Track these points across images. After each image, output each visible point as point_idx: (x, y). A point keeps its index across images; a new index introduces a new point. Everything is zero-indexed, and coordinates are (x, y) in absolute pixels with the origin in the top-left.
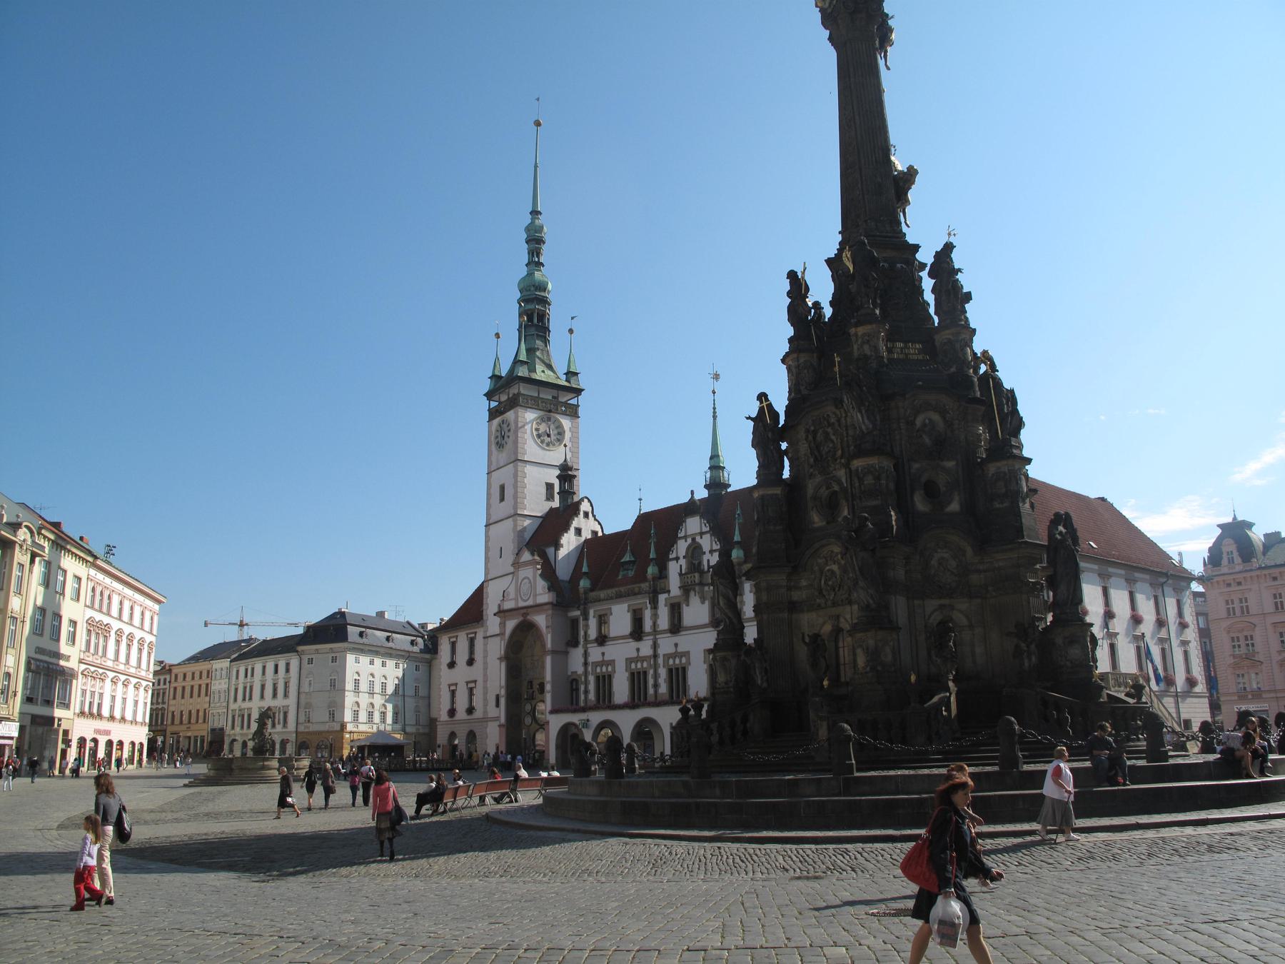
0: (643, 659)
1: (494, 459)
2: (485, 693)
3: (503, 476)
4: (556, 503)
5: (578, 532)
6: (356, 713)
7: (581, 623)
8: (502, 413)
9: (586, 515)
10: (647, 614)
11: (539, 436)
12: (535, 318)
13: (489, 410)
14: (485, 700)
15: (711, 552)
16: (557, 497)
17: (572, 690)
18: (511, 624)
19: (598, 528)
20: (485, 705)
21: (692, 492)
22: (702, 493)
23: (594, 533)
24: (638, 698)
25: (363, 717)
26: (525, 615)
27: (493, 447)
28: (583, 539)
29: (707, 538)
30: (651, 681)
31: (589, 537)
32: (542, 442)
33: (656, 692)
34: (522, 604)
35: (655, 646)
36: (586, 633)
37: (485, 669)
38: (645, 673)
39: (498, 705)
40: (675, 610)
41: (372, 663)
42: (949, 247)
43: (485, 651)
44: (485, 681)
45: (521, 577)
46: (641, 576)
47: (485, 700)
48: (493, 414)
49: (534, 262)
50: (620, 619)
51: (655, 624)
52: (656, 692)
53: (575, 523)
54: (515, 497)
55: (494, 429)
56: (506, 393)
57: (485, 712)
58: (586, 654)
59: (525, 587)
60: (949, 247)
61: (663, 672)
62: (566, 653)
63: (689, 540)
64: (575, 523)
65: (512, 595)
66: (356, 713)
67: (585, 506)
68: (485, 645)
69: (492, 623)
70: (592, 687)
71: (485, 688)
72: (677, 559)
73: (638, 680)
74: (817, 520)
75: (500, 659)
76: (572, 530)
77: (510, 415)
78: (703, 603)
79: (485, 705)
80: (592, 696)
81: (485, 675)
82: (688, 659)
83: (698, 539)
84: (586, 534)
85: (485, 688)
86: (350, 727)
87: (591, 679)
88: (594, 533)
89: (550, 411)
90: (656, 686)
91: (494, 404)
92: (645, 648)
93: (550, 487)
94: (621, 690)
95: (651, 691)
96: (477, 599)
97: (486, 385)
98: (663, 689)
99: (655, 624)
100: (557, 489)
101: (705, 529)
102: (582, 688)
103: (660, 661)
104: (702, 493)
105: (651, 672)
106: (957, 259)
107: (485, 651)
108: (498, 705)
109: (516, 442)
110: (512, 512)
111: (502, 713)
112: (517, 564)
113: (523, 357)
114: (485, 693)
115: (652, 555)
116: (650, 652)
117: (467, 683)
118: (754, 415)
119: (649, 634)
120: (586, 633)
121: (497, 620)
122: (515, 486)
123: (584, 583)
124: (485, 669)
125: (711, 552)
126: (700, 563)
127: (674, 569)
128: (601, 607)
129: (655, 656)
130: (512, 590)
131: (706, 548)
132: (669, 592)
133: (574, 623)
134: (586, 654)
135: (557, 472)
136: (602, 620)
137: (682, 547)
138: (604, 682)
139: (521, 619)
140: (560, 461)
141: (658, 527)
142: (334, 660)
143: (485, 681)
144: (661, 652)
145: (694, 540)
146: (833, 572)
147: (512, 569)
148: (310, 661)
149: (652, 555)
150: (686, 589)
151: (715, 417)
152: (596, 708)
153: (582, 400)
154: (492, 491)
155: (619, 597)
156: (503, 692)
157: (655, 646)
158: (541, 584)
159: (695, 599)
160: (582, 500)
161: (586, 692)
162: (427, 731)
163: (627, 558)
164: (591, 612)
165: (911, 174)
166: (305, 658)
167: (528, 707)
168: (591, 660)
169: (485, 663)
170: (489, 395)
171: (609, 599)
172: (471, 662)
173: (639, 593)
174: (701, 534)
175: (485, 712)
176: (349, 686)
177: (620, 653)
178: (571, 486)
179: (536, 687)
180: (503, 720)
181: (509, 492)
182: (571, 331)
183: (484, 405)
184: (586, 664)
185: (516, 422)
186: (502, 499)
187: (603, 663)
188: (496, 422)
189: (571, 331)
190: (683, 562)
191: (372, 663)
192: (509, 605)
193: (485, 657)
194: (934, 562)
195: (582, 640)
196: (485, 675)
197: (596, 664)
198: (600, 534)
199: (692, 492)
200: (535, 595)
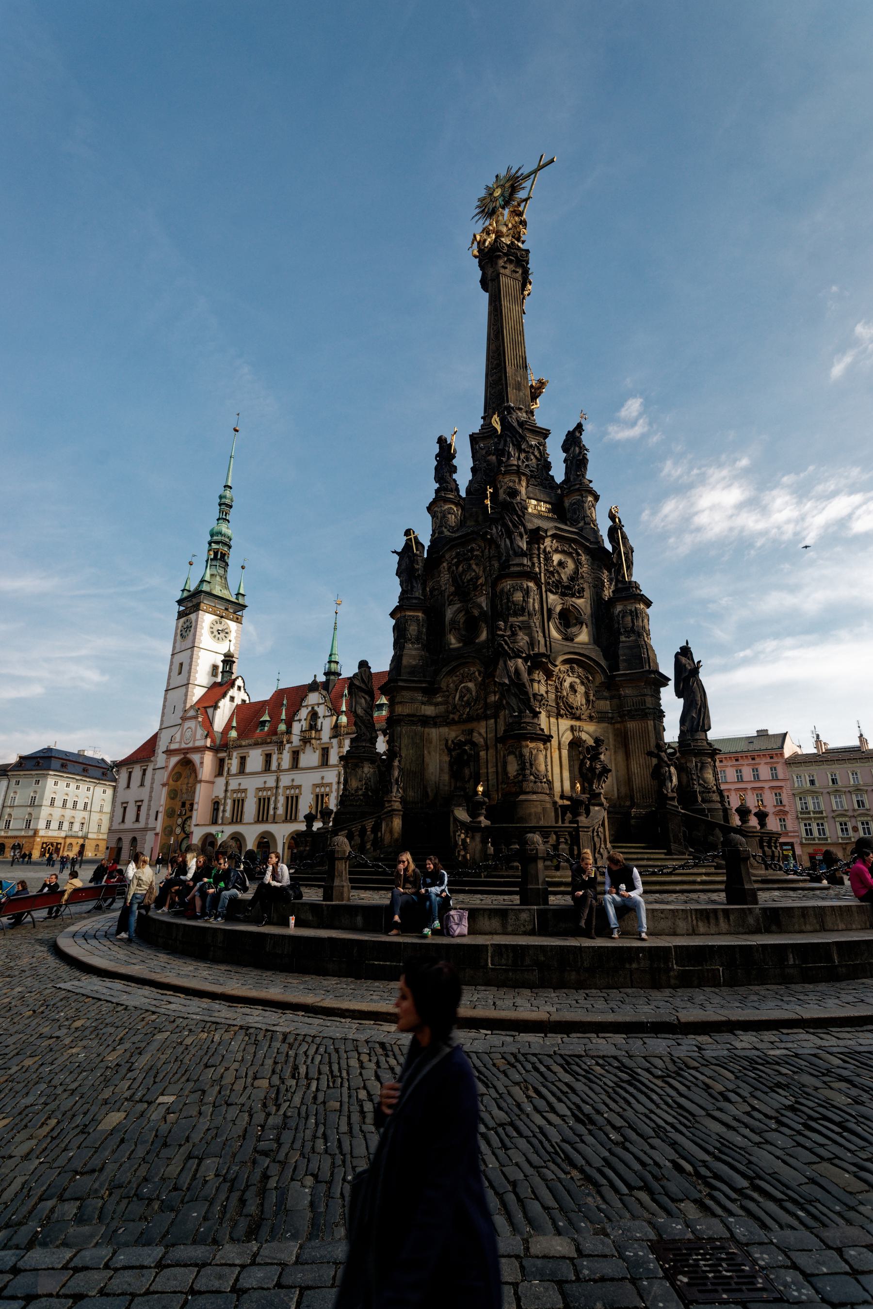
0: (270, 789)
1: (178, 645)
2: (149, 810)
3: (182, 657)
4: (219, 679)
5: (232, 699)
6: (49, 823)
7: (226, 761)
8: (187, 615)
9: (239, 688)
10: (274, 758)
11: (212, 633)
12: (219, 555)
13: (179, 612)
14: (148, 815)
15: (324, 717)
16: (220, 675)
17: (214, 809)
18: (174, 760)
19: (246, 698)
20: (147, 819)
21: (315, 676)
22: (322, 678)
23: (244, 701)
24: (262, 816)
25: (54, 825)
26: (187, 753)
27: (179, 637)
28: (235, 704)
29: (322, 707)
30: (272, 806)
31: (240, 703)
32: (215, 637)
33: (275, 813)
34: (184, 746)
35: (278, 780)
36: (229, 769)
37: (151, 792)
38: (269, 799)
41: (68, 786)
42: (579, 427)
43: (153, 779)
44: (150, 801)
45: (186, 727)
46: (274, 732)
47: (148, 815)
48: (181, 615)
49: (223, 518)
50: (255, 759)
51: (279, 764)
52: (275, 813)
54: (189, 672)
55: (180, 625)
56: (191, 603)
57: (147, 823)
58: (227, 784)
59: (188, 734)
60: (579, 427)
62: (213, 783)
63: (310, 708)
64: (231, 693)
65: (178, 740)
66: (49, 823)
67: (239, 682)
68: (154, 775)
69: (160, 759)
70: (229, 808)
71: (149, 805)
72: (300, 720)
73: (263, 804)
74: (454, 642)
75: (164, 785)
76: (228, 698)
77: (193, 616)
79: (147, 819)
80: (228, 814)
81: (151, 797)
82: (300, 791)
83: (316, 708)
84: (238, 701)
85: (149, 805)
86: (41, 833)
87: (229, 802)
88: (244, 701)
89: (222, 617)
90: (275, 808)
91: (182, 608)
92: (271, 781)
93: (215, 667)
94: (250, 808)
95: (271, 812)
96: (153, 741)
97: (178, 595)
98: (281, 811)
99: (279, 764)
100: (220, 669)
101: (321, 701)
102: (221, 808)
103: (280, 791)
104: (322, 678)
105: (273, 798)
106: (586, 439)
107: (153, 779)
109: (195, 635)
110: (186, 682)
111: (159, 826)
112: (184, 719)
113: (207, 578)
114: (149, 810)
115: (283, 717)
116: (273, 784)
117: (136, 802)
118: (399, 550)
119: (275, 772)
120: (229, 769)
121: (164, 756)
122: (190, 665)
123: (234, 734)
124: (151, 792)
126: (316, 725)
127: (296, 728)
128: (242, 752)
129: (277, 787)
130: (178, 737)
131: (321, 714)
133: (221, 762)
134: (227, 784)
135: (222, 658)
136: (243, 760)
137: (304, 713)
138: (239, 804)
139: (183, 756)
140: (225, 651)
141: (291, 698)
142: (38, 782)
143: (150, 801)
144: (281, 784)
145: (313, 708)
146: (468, 689)
147: (180, 721)
148: (18, 783)
149: (283, 717)
150: (306, 741)
151: (335, 629)
152: (232, 822)
153: (245, 612)
154: (173, 667)
155: (256, 744)
156: (161, 809)
157: (278, 780)
158: (200, 732)
159: (308, 749)
160: (237, 678)
161: (224, 811)
162: (105, 837)
163: (266, 718)
164: (235, 754)
165: (542, 384)
166: (13, 781)
167: (180, 821)
168: (230, 788)
169: (152, 788)
170: (180, 602)
171: (249, 746)
172: (142, 785)
173: (270, 743)
174: (319, 704)
175: (147, 823)
176: (47, 802)
177: (251, 784)
178: (231, 668)
179: (188, 806)
180: (159, 829)
181: (185, 668)
182: (243, 568)
183: (176, 608)
184: (226, 791)
185: (197, 621)
186: (180, 673)
187: (239, 791)
188: (182, 620)
189: (243, 568)
190: (303, 723)
191: (68, 786)
192: (173, 747)
193: (152, 783)
194: (567, 684)
195: (225, 774)
196: (151, 797)
197: (234, 791)
198: (248, 702)
199: (315, 676)
200: (194, 741)
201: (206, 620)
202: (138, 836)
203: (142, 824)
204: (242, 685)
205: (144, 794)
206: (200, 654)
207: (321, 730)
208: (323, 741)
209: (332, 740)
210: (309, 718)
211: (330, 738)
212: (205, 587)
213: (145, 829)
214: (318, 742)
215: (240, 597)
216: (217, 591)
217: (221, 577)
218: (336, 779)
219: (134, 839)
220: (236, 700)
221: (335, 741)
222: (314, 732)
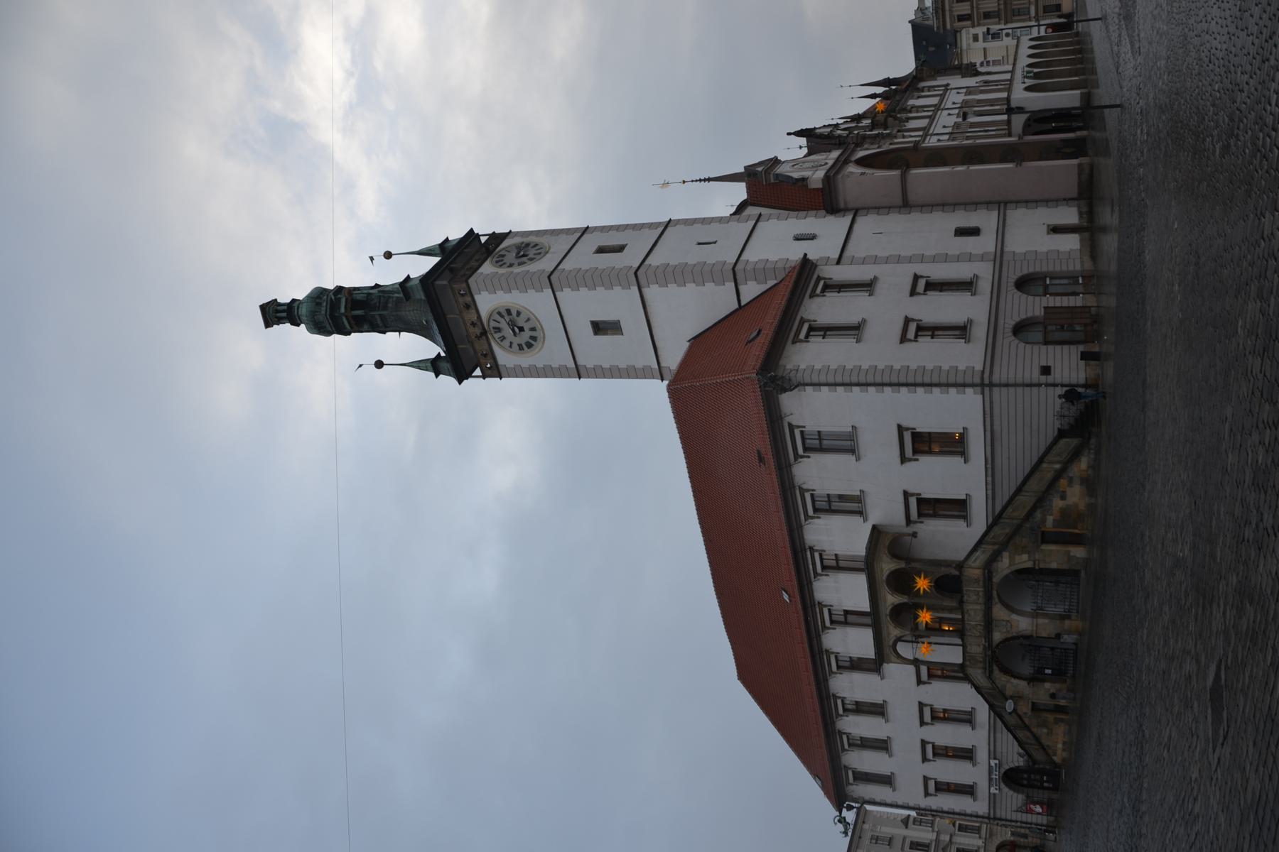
2: (946, 258)
20: (970, 258)
37: (899, 260)
39: (974, 232)
44: (922, 259)
47: (958, 259)
57: (982, 258)
68: (853, 261)
71: (934, 259)
79: (970, 258)
81: (910, 260)
85: (934, 259)
108: (974, 232)
114: (946, 258)
143: (922, 259)
175: (982, 258)
196: (910, 260)
202: (1012, 275)
203: (984, 271)
205: (895, 279)
213: (999, 258)
219: (1023, 284)
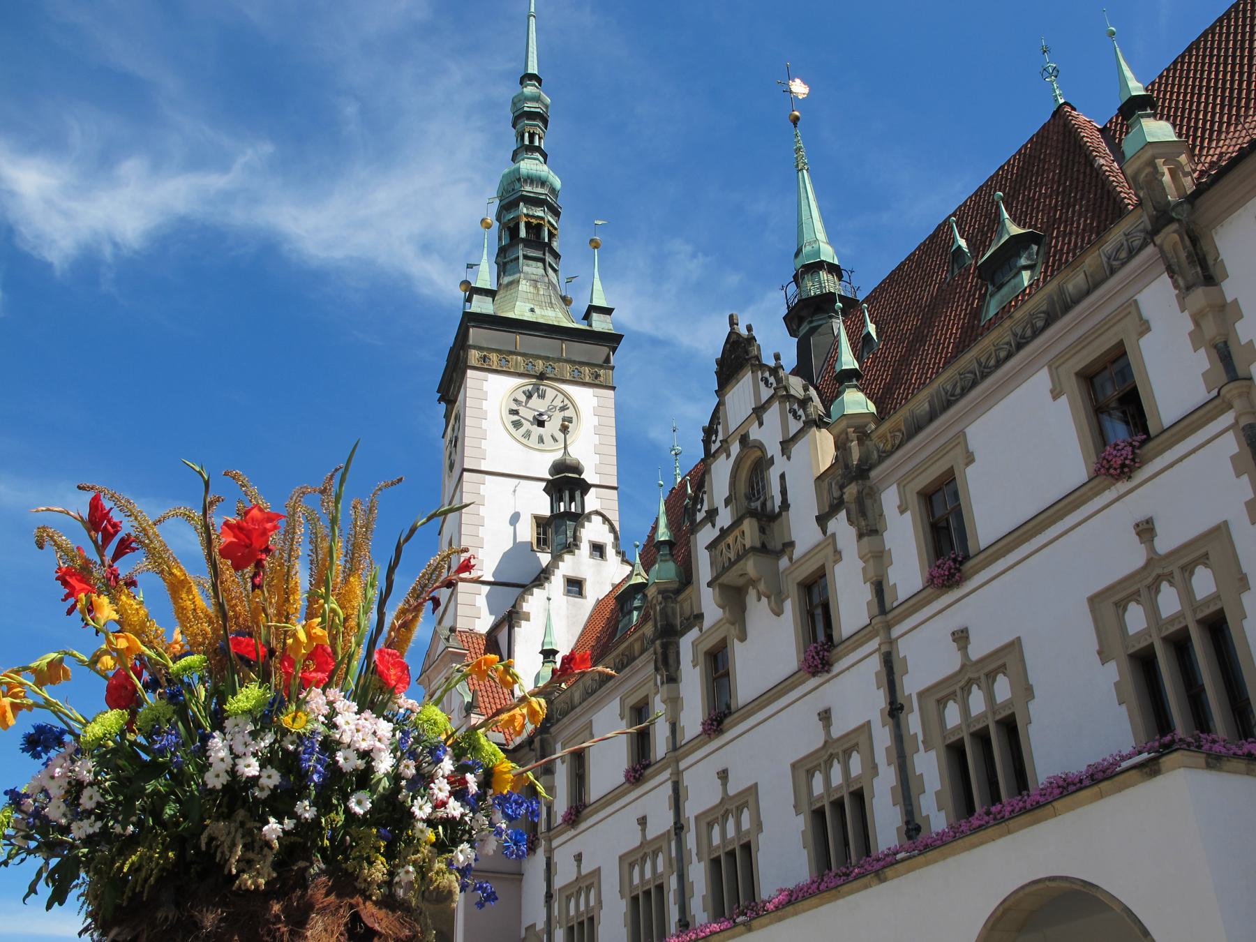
5: (575, 586)
9: (598, 549)
10: (659, 707)
11: (517, 425)
28: (586, 605)
38: (660, 888)
40: (717, 665)
53: (568, 566)
61: (698, 874)
63: (735, 448)
67: (594, 531)
72: (712, 514)
78: (778, 612)
83: (755, 433)
89: (542, 377)
105: (673, 883)
125: (787, 445)
129: (679, 828)
131: (773, 449)
132: (700, 617)
145: (744, 440)
168: (558, 882)
174: (759, 411)
184: (549, 896)
201: (491, 393)
204: (607, 538)
206: (483, 490)
207: (785, 505)
208: (798, 551)
209: (832, 525)
210: (742, 488)
211: (822, 520)
212: (481, 305)
214: (784, 562)
215: (595, 316)
216: (520, 310)
217: (535, 282)
218: (880, 700)
220: (588, 588)
221: (840, 525)
222: (749, 526)
